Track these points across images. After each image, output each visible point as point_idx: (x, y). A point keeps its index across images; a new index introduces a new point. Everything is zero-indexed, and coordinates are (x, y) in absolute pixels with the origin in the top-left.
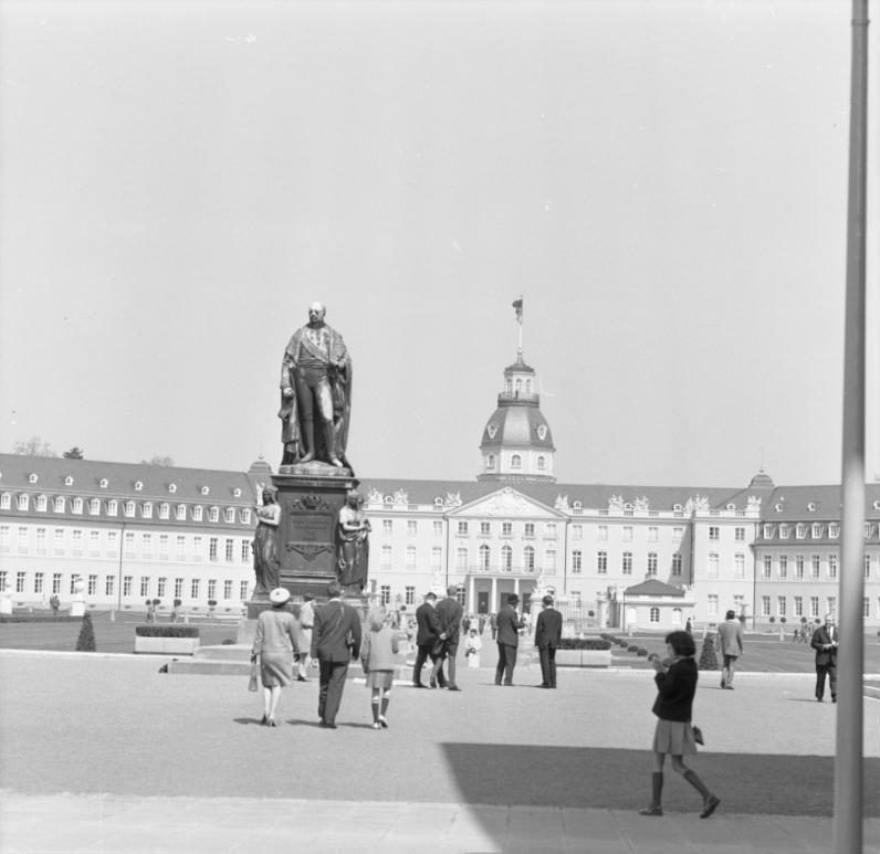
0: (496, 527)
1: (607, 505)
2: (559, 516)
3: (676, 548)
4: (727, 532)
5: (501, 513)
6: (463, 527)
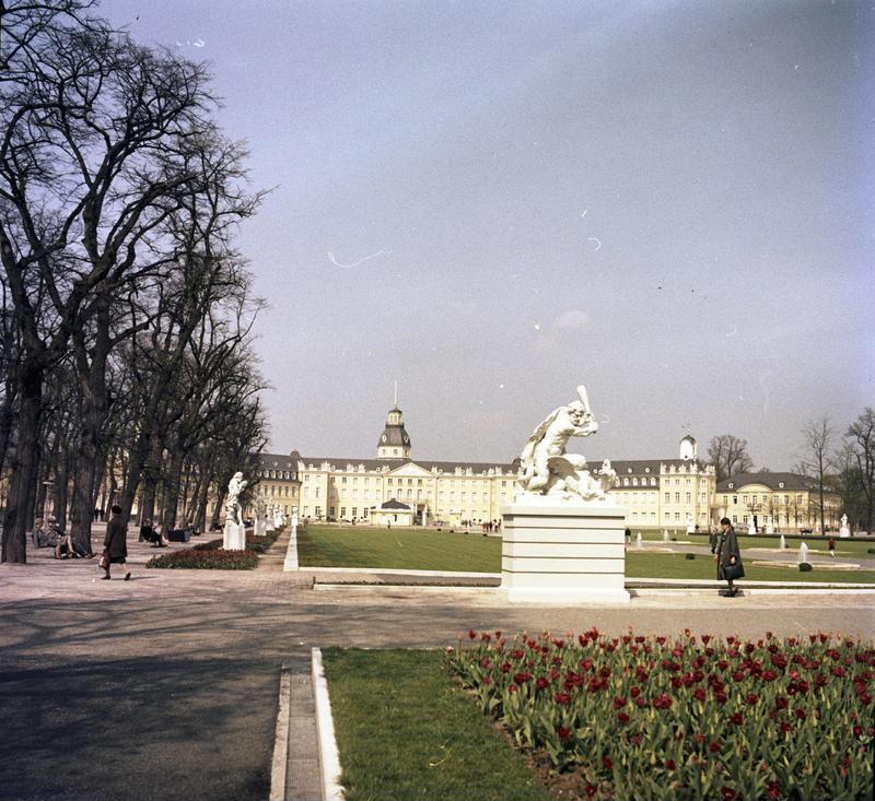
0: (405, 481)
6: (390, 481)
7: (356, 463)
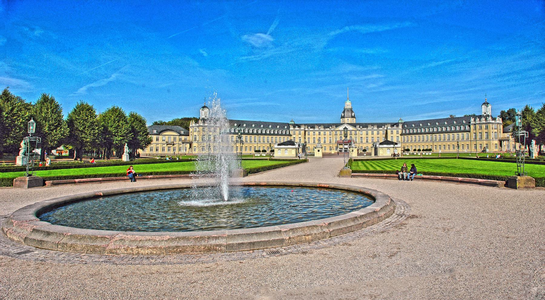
7: (319, 125)
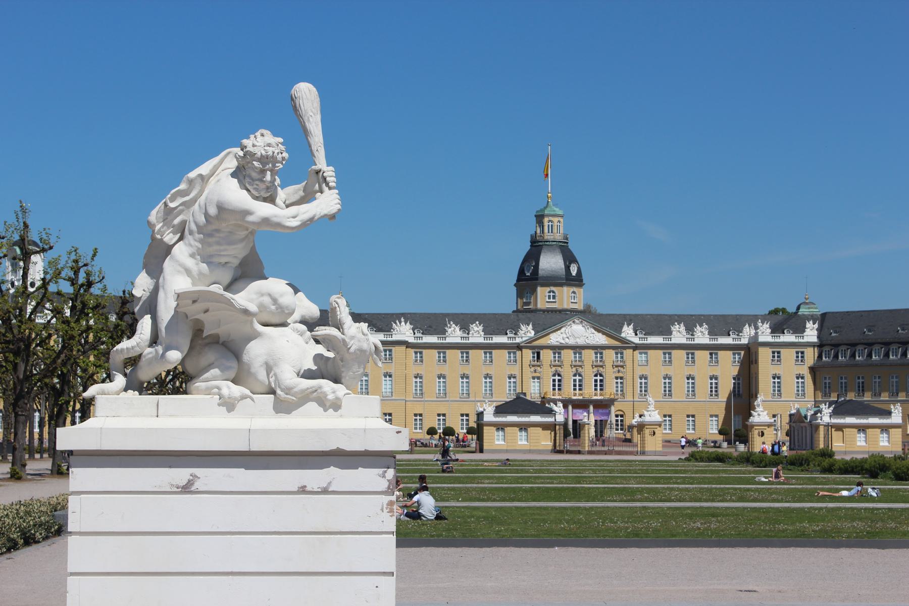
1: (670, 333)
2: (625, 345)
3: (735, 371)
4: (788, 355)
5: (571, 342)
